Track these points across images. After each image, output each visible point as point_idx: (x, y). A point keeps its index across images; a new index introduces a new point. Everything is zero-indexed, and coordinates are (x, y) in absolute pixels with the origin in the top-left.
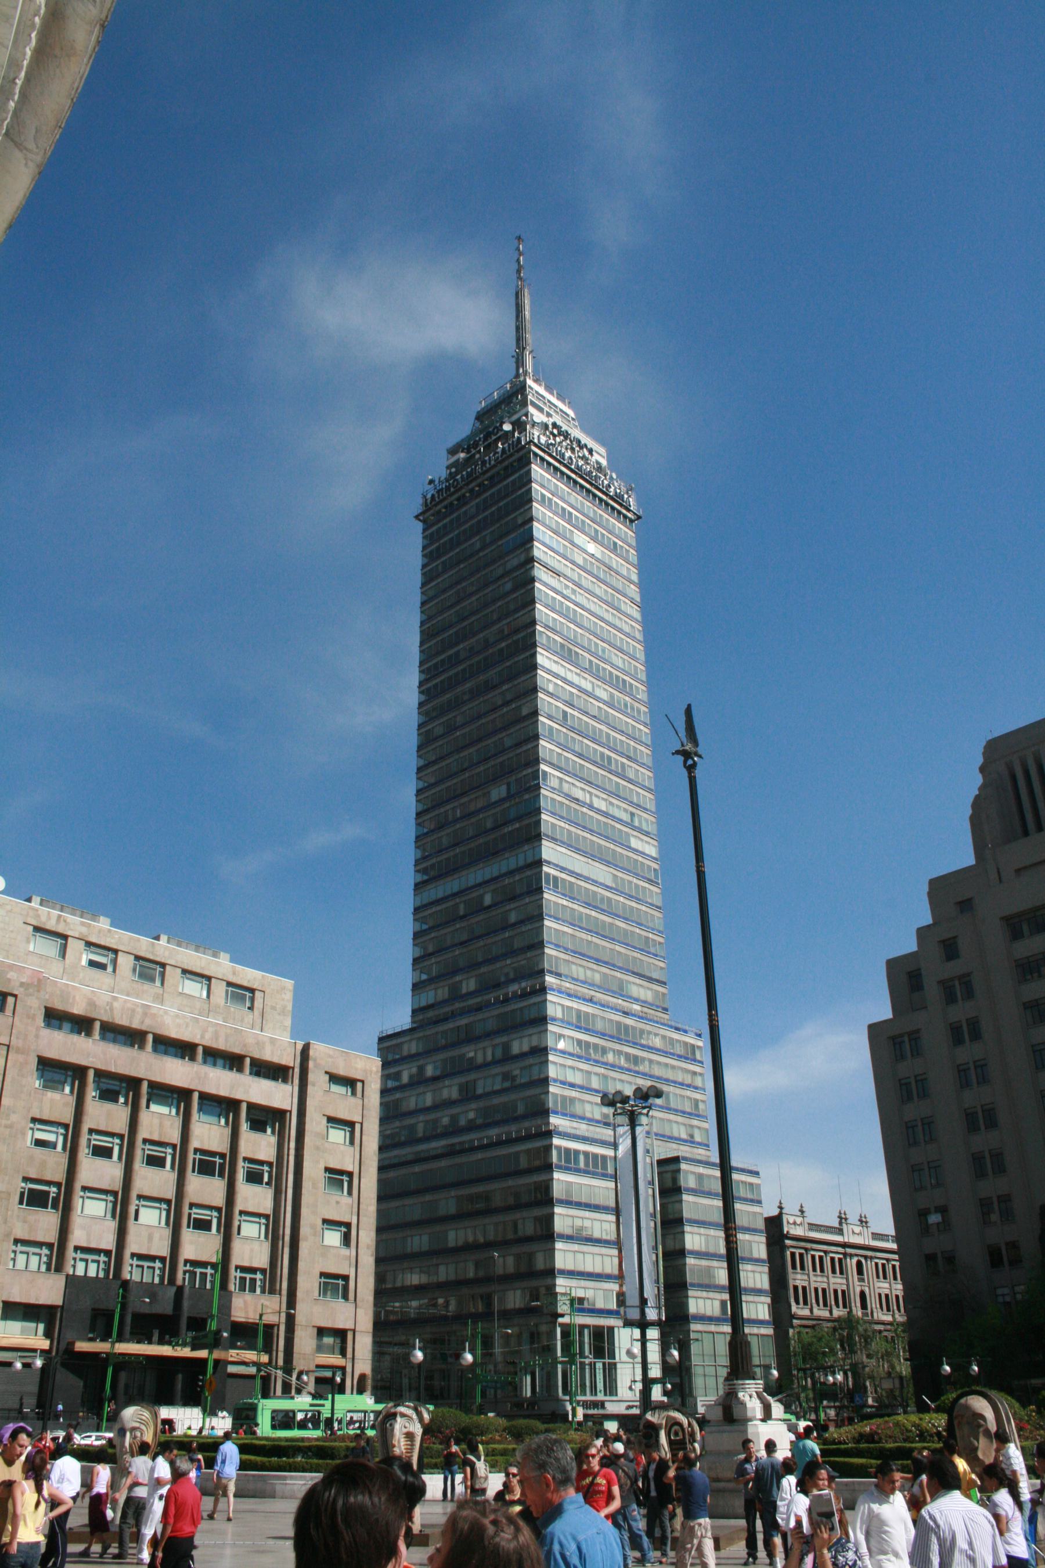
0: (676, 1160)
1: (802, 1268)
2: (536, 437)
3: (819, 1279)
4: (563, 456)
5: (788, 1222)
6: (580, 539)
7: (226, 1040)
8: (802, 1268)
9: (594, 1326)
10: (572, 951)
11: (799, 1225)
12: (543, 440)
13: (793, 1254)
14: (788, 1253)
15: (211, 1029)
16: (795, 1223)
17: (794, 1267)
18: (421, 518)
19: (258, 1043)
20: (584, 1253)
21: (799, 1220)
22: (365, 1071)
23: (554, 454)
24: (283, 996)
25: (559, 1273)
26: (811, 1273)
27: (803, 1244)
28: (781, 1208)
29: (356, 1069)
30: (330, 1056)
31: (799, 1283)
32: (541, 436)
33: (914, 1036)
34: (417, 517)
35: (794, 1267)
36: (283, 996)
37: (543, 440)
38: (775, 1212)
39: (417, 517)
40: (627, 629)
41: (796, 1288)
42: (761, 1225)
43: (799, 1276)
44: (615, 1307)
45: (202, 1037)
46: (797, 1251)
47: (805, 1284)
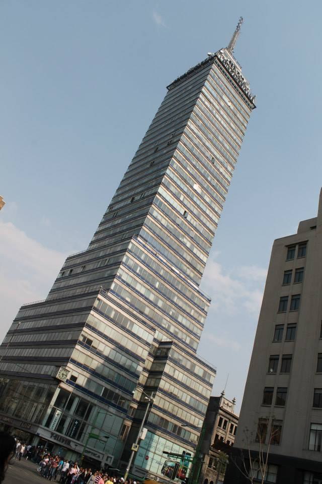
0: (171, 343)
1: (224, 428)
3: (232, 437)
4: (229, 69)
5: (224, 403)
6: (224, 97)
8: (224, 428)
9: (83, 398)
10: (157, 234)
11: (230, 407)
13: (221, 419)
14: (218, 418)
16: (228, 404)
17: (220, 425)
18: (169, 88)
20: (93, 359)
21: (230, 404)
25: (71, 361)
26: (228, 433)
27: (228, 416)
28: (223, 394)
31: (219, 434)
33: (303, 245)
34: (167, 87)
35: (220, 425)
37: (222, 60)
38: (219, 395)
39: (167, 87)
41: (217, 436)
42: (209, 398)
43: (221, 431)
44: (101, 395)
46: (224, 419)
47: (223, 436)
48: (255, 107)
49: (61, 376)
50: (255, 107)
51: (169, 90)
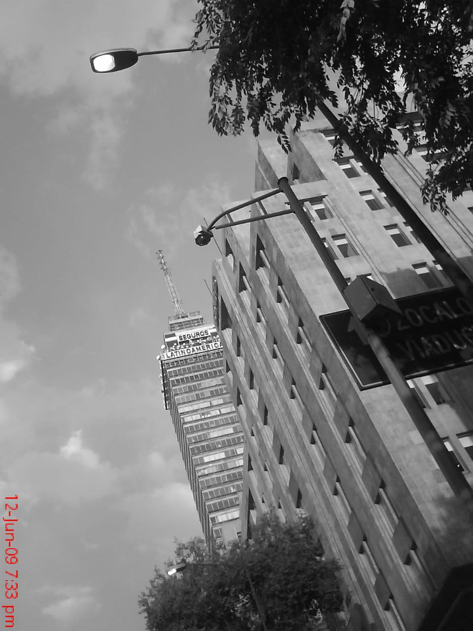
23: (179, 356)
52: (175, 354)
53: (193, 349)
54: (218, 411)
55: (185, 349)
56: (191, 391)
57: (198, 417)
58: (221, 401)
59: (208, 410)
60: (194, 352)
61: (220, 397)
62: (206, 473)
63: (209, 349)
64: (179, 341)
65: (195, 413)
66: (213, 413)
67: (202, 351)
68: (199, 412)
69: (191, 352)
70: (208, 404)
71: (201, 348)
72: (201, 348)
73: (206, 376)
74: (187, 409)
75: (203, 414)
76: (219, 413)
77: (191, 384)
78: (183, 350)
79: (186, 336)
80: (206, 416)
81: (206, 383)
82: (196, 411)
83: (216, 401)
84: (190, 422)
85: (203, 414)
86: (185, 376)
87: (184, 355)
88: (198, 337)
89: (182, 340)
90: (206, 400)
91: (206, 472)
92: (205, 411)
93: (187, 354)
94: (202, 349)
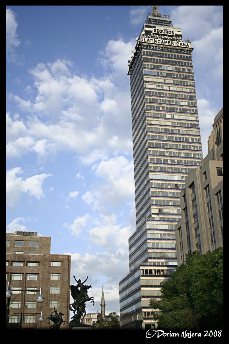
2: (143, 39)
7: (18, 258)
12: (146, 39)
15: (13, 256)
18: (130, 74)
19: (28, 257)
22: (63, 259)
23: (152, 42)
24: (48, 241)
29: (60, 259)
30: (50, 257)
32: (145, 38)
34: (128, 74)
36: (48, 241)
40: (188, 91)
45: (10, 259)
48: (193, 49)
49: (140, 318)
50: (193, 49)
51: (131, 75)
52: (150, 40)
53: (162, 41)
54: (168, 87)
55: (157, 40)
56: (154, 69)
57: (155, 87)
58: (172, 82)
59: (162, 85)
60: (162, 44)
61: (172, 79)
62: (152, 123)
63: (172, 45)
64: (153, 32)
65: (154, 84)
66: (165, 88)
67: (168, 44)
68: (156, 84)
69: (161, 43)
70: (163, 81)
71: (168, 42)
72: (168, 42)
73: (166, 63)
74: (149, 80)
75: (159, 86)
76: (168, 89)
77: (156, 64)
78: (155, 39)
79: (159, 30)
80: (160, 88)
81: (165, 67)
82: (155, 82)
83: (169, 81)
84: (149, 89)
85: (159, 86)
86: (153, 58)
87: (155, 43)
88: (167, 34)
89: (155, 32)
90: (163, 78)
91: (152, 122)
92: (160, 85)
93: (157, 43)
94: (168, 43)
